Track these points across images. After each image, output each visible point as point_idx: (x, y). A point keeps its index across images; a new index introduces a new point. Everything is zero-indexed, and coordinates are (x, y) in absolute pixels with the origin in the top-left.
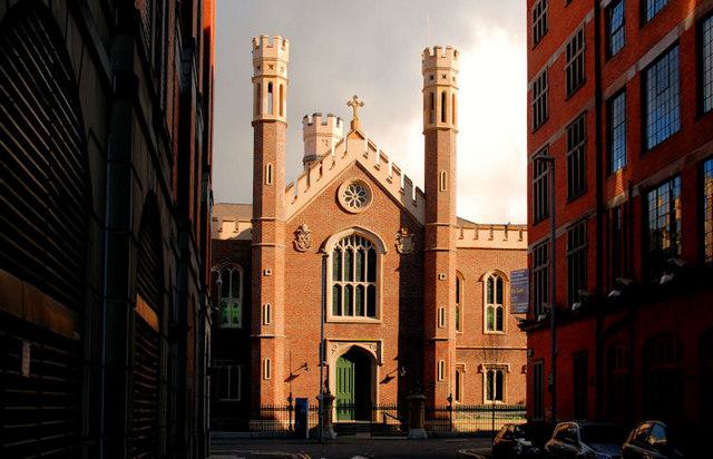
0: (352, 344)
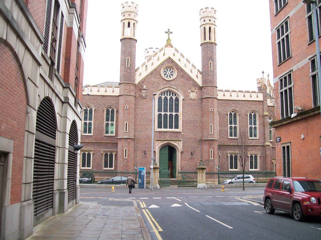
0: (167, 142)
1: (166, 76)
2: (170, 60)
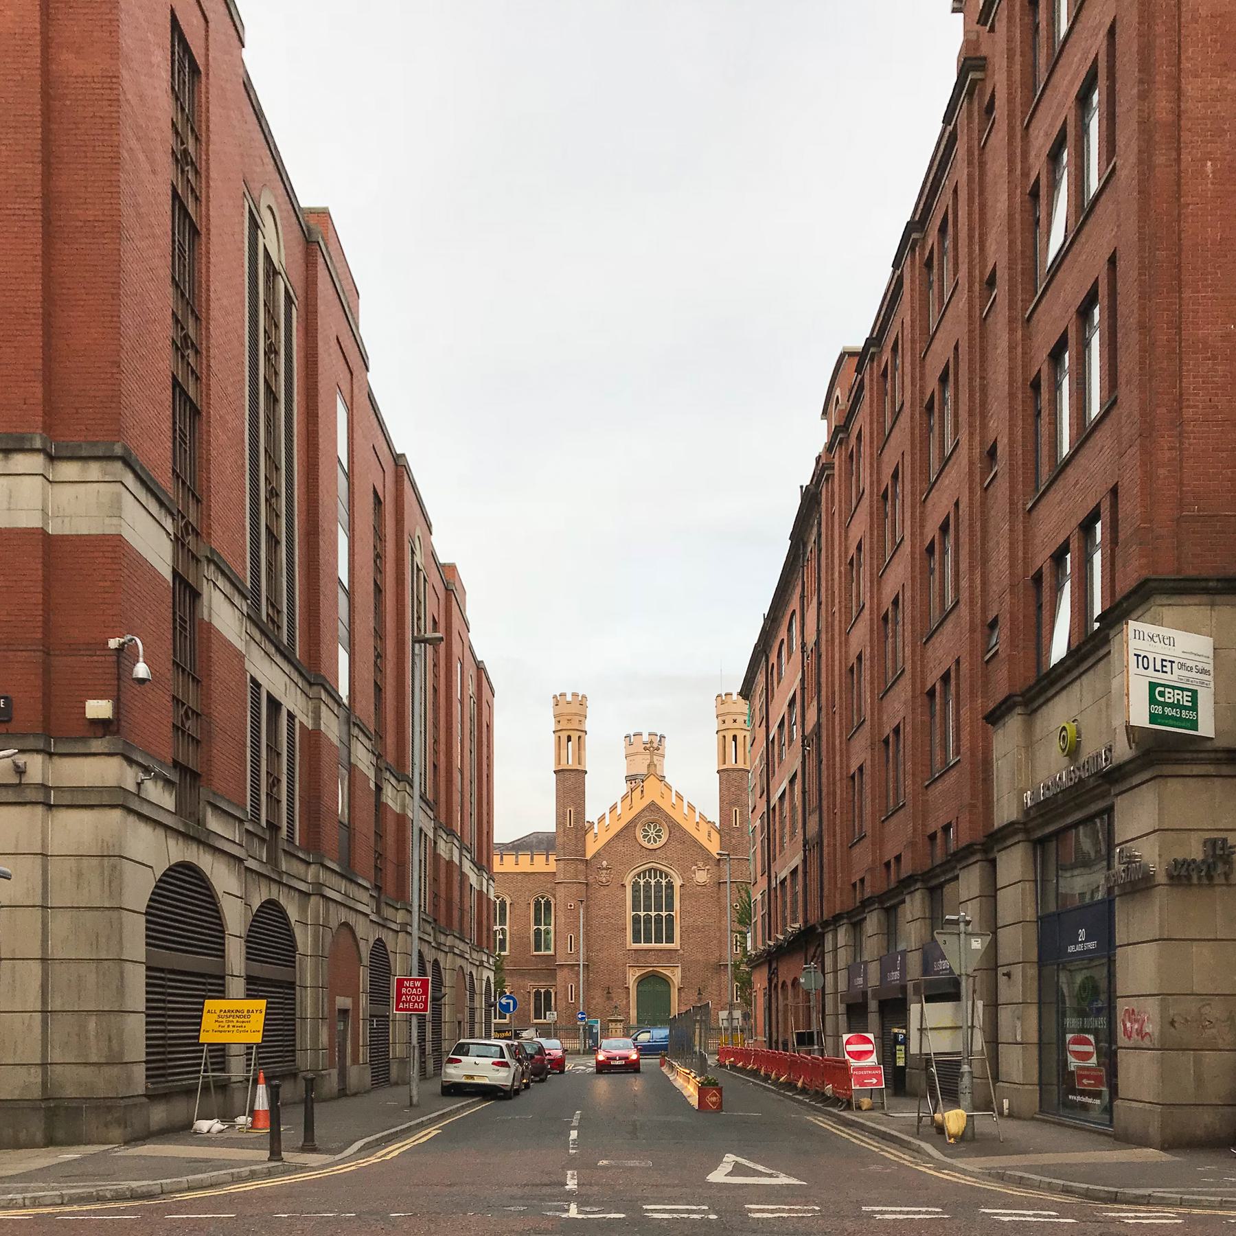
2: (653, 807)
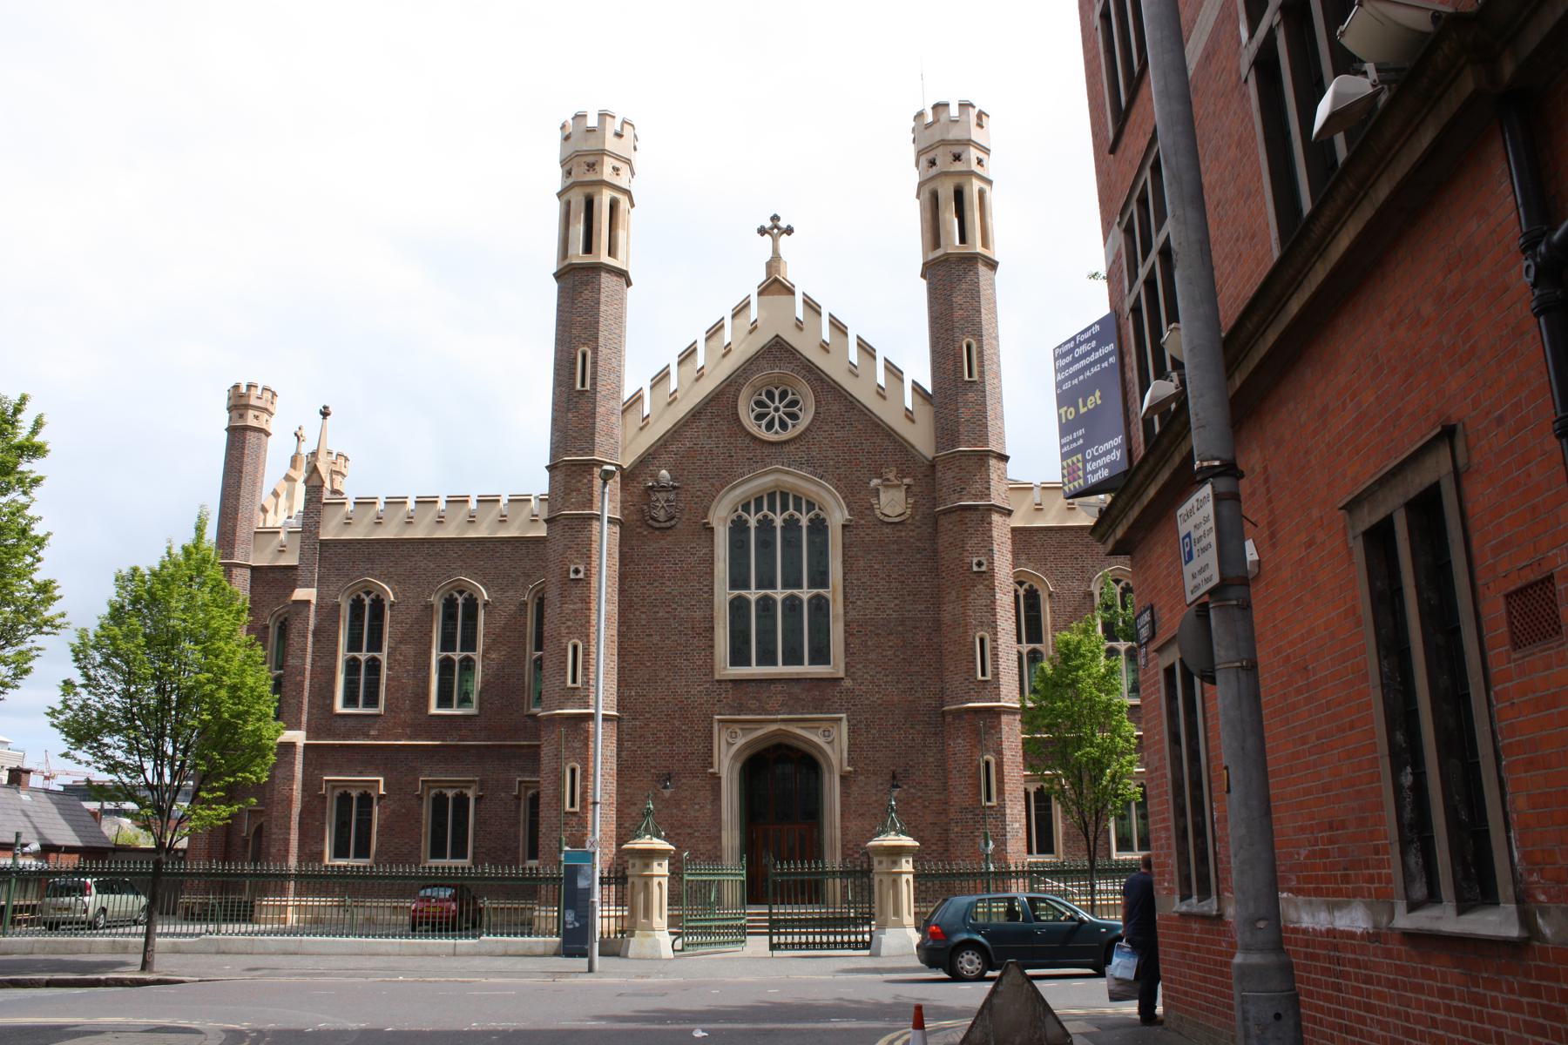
1: (764, 423)
2: (778, 350)
